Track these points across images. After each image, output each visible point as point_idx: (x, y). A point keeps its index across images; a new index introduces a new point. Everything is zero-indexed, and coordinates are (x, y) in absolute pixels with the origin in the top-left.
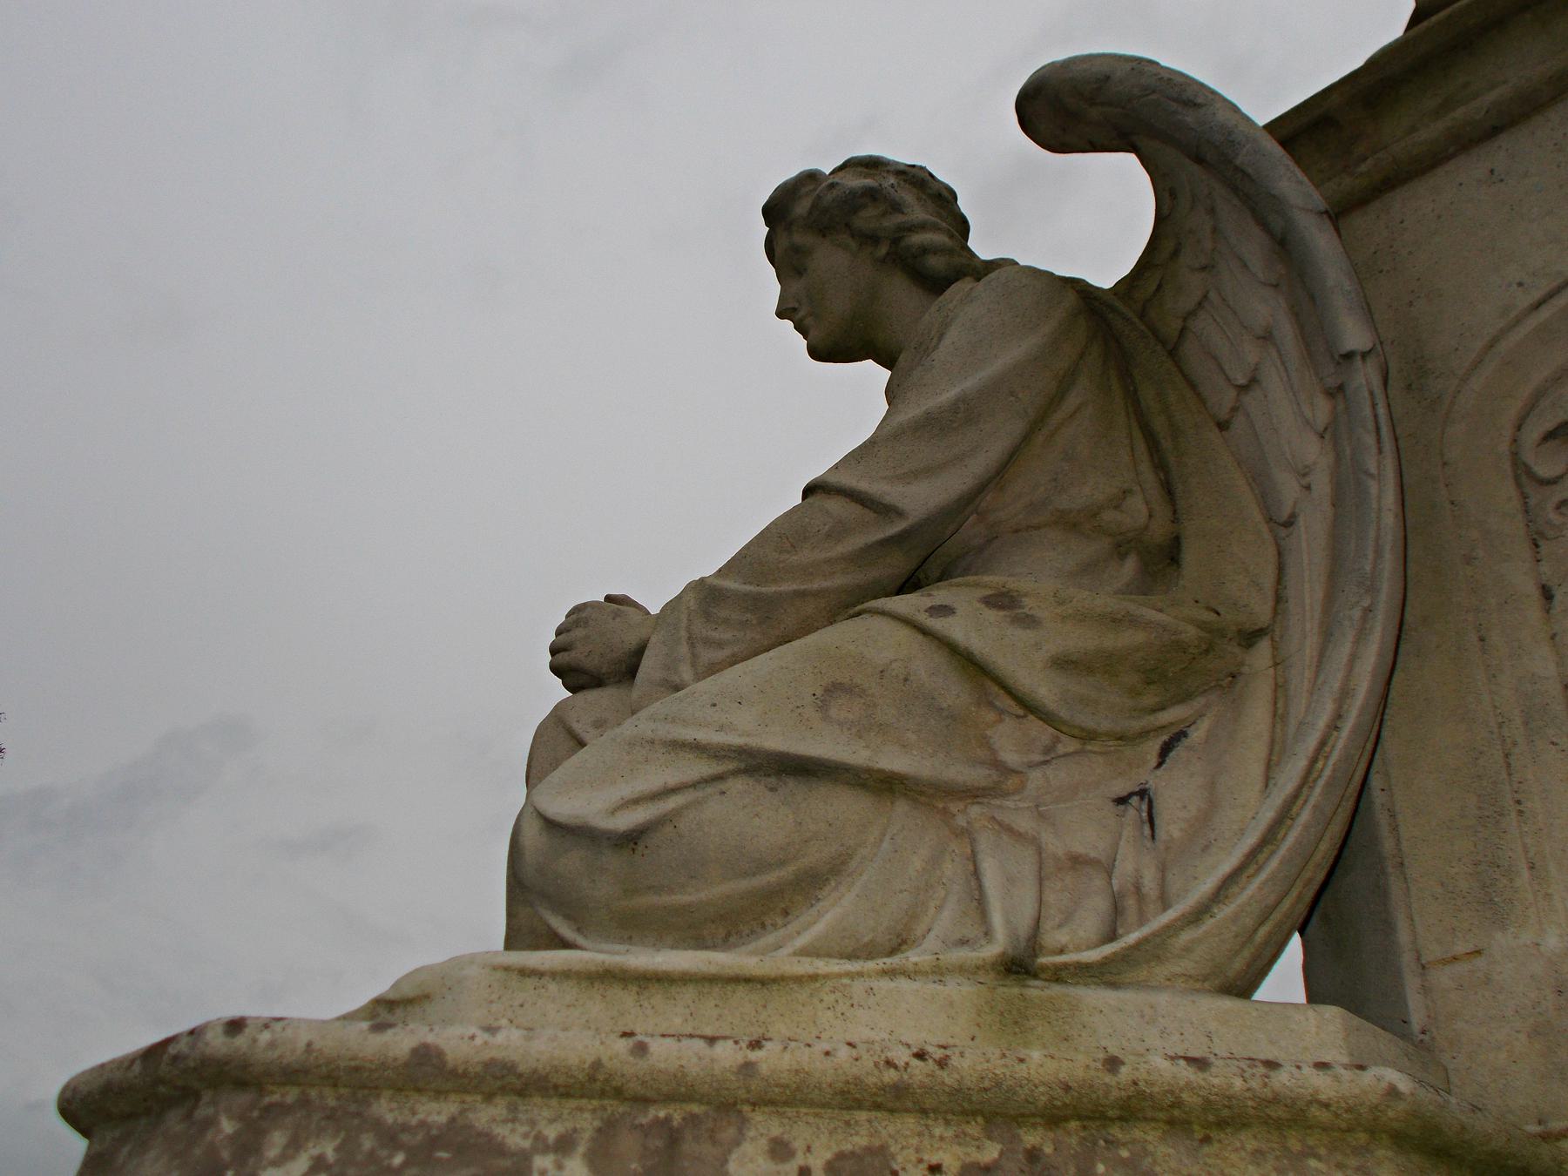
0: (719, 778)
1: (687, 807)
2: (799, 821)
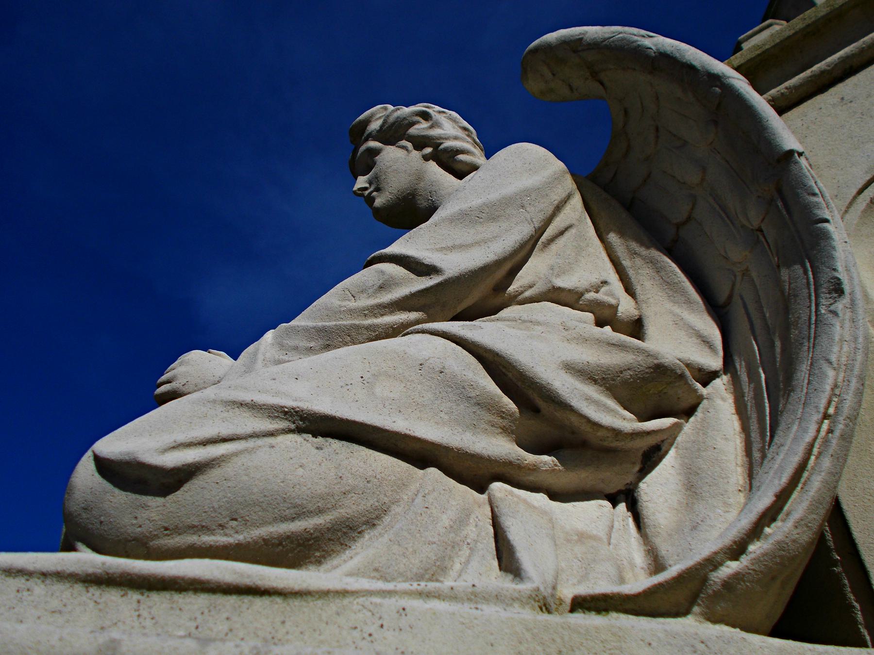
0: (272, 434)
1: (236, 454)
2: (341, 475)
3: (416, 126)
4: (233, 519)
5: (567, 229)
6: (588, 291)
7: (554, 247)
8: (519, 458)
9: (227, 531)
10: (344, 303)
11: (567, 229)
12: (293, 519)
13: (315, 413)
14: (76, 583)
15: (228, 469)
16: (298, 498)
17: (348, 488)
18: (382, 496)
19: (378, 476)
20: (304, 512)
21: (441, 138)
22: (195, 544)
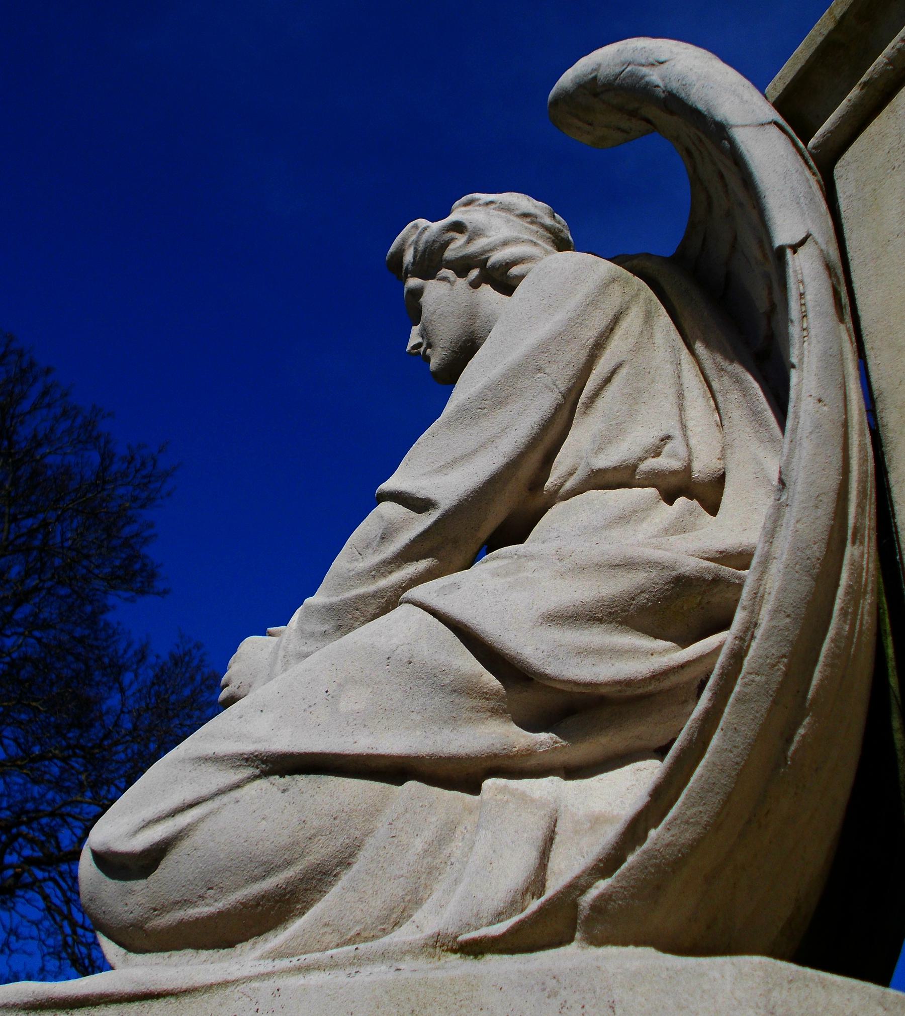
0: (237, 786)
1: (202, 820)
2: (304, 819)
3: (452, 246)
4: (209, 889)
5: (614, 372)
6: (642, 459)
7: (601, 403)
8: (505, 747)
9: (207, 901)
10: (351, 566)
11: (614, 372)
12: (264, 877)
13: (273, 754)
14: (19, 1011)
15: (197, 838)
16: (263, 856)
17: (313, 832)
18: (352, 831)
19: (346, 810)
20: (273, 868)
21: (486, 252)
22: (183, 919)
